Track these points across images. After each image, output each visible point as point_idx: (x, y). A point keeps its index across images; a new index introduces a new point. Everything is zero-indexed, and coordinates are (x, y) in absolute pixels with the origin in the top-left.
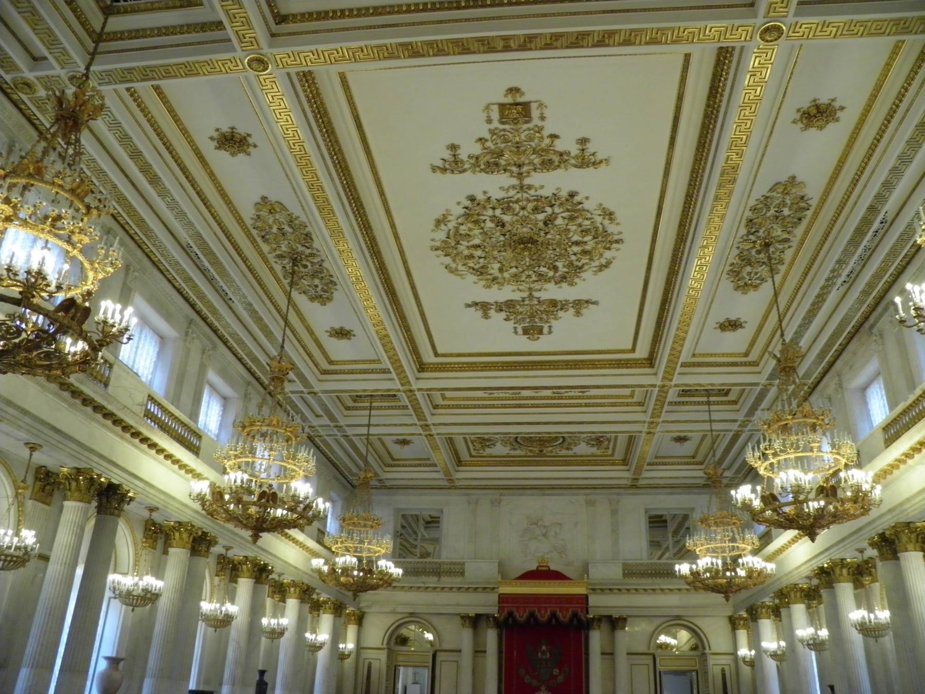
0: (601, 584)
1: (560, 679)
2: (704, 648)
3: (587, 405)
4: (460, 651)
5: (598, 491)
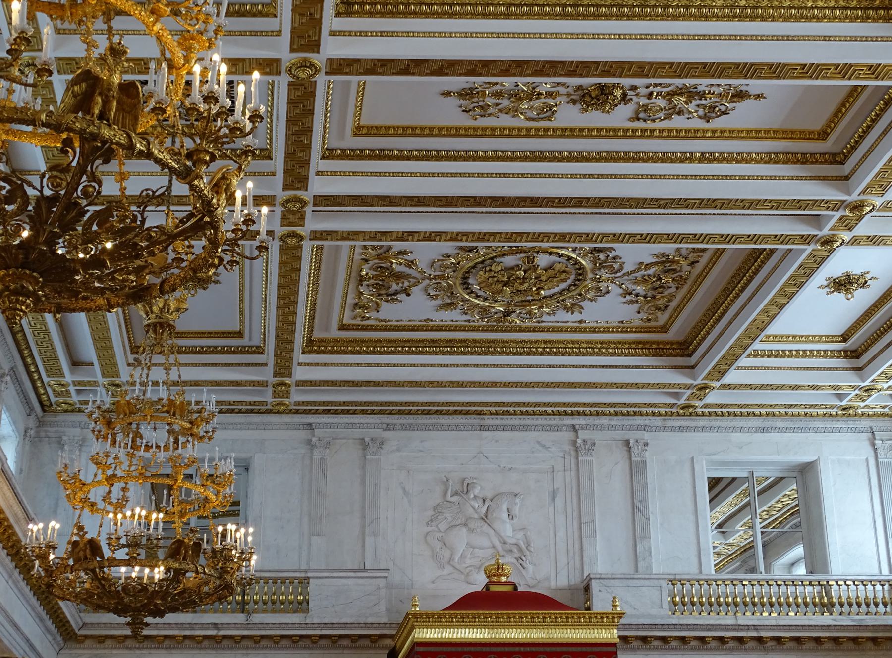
3: (704, 158)
5: (604, 421)
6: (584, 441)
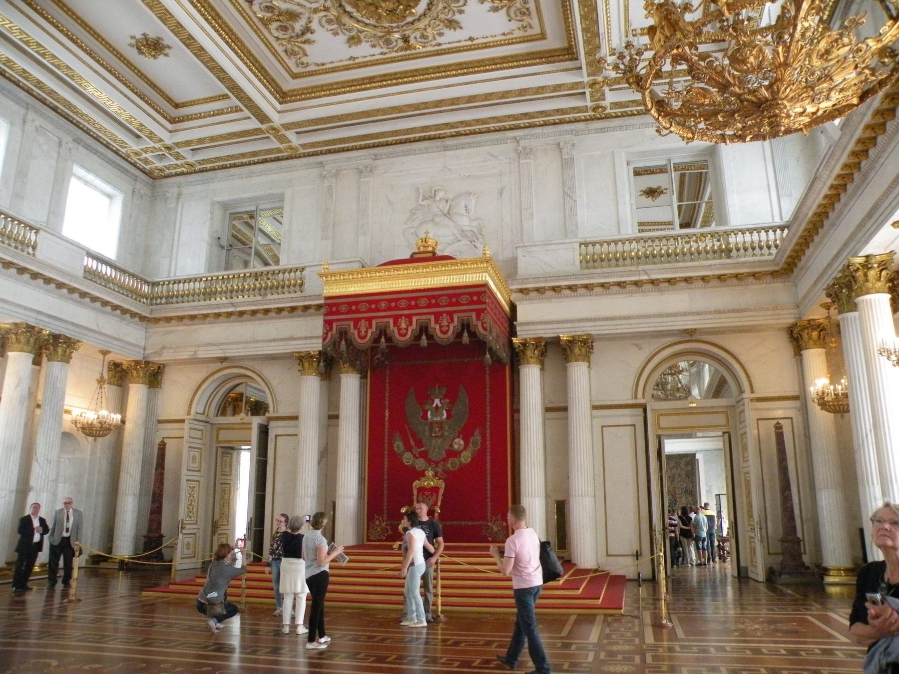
0: (537, 279)
1: (466, 457)
2: (741, 392)
4: (296, 418)
5: (538, 130)
6: (525, 148)
